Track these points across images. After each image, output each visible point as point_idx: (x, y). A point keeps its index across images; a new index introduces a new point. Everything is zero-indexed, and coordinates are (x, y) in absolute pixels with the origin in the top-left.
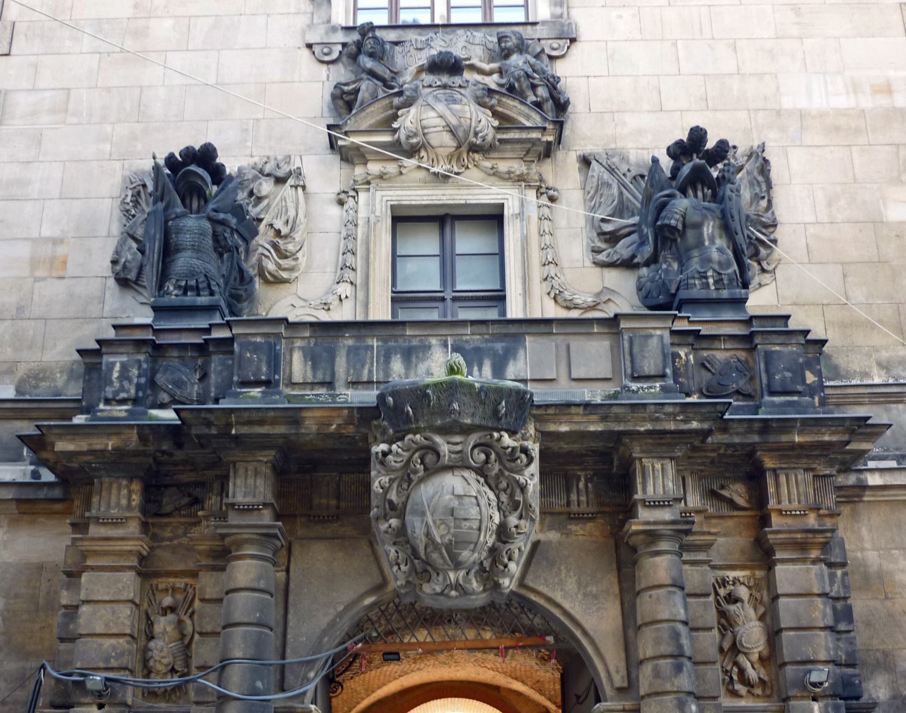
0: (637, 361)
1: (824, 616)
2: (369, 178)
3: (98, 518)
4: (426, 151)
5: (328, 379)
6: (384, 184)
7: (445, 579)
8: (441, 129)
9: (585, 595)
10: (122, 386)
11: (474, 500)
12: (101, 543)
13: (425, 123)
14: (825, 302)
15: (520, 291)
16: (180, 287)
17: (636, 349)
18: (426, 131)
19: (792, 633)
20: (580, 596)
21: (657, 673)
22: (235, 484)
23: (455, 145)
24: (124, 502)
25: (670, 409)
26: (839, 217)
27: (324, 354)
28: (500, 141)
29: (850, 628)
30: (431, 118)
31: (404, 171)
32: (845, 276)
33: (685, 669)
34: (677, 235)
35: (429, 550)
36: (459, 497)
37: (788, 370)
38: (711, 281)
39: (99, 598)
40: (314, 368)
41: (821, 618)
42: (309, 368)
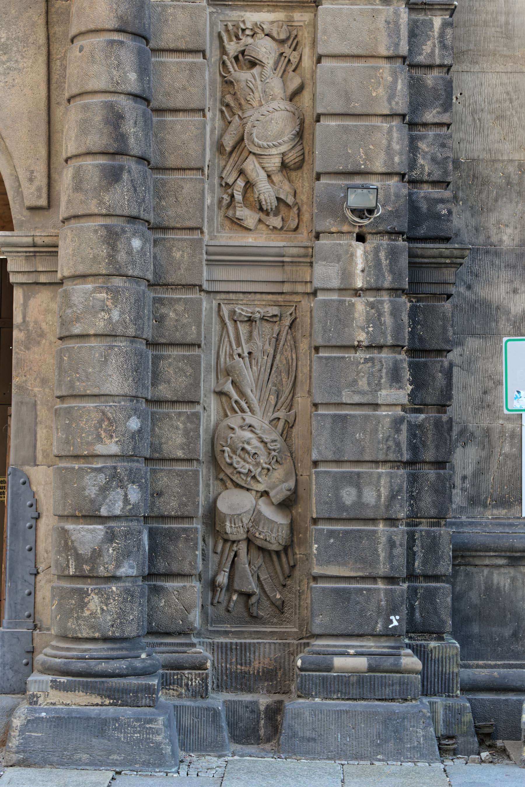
1: (391, 97)
19: (333, 123)
29: (445, 118)
33: (125, 176)
41: (385, 98)
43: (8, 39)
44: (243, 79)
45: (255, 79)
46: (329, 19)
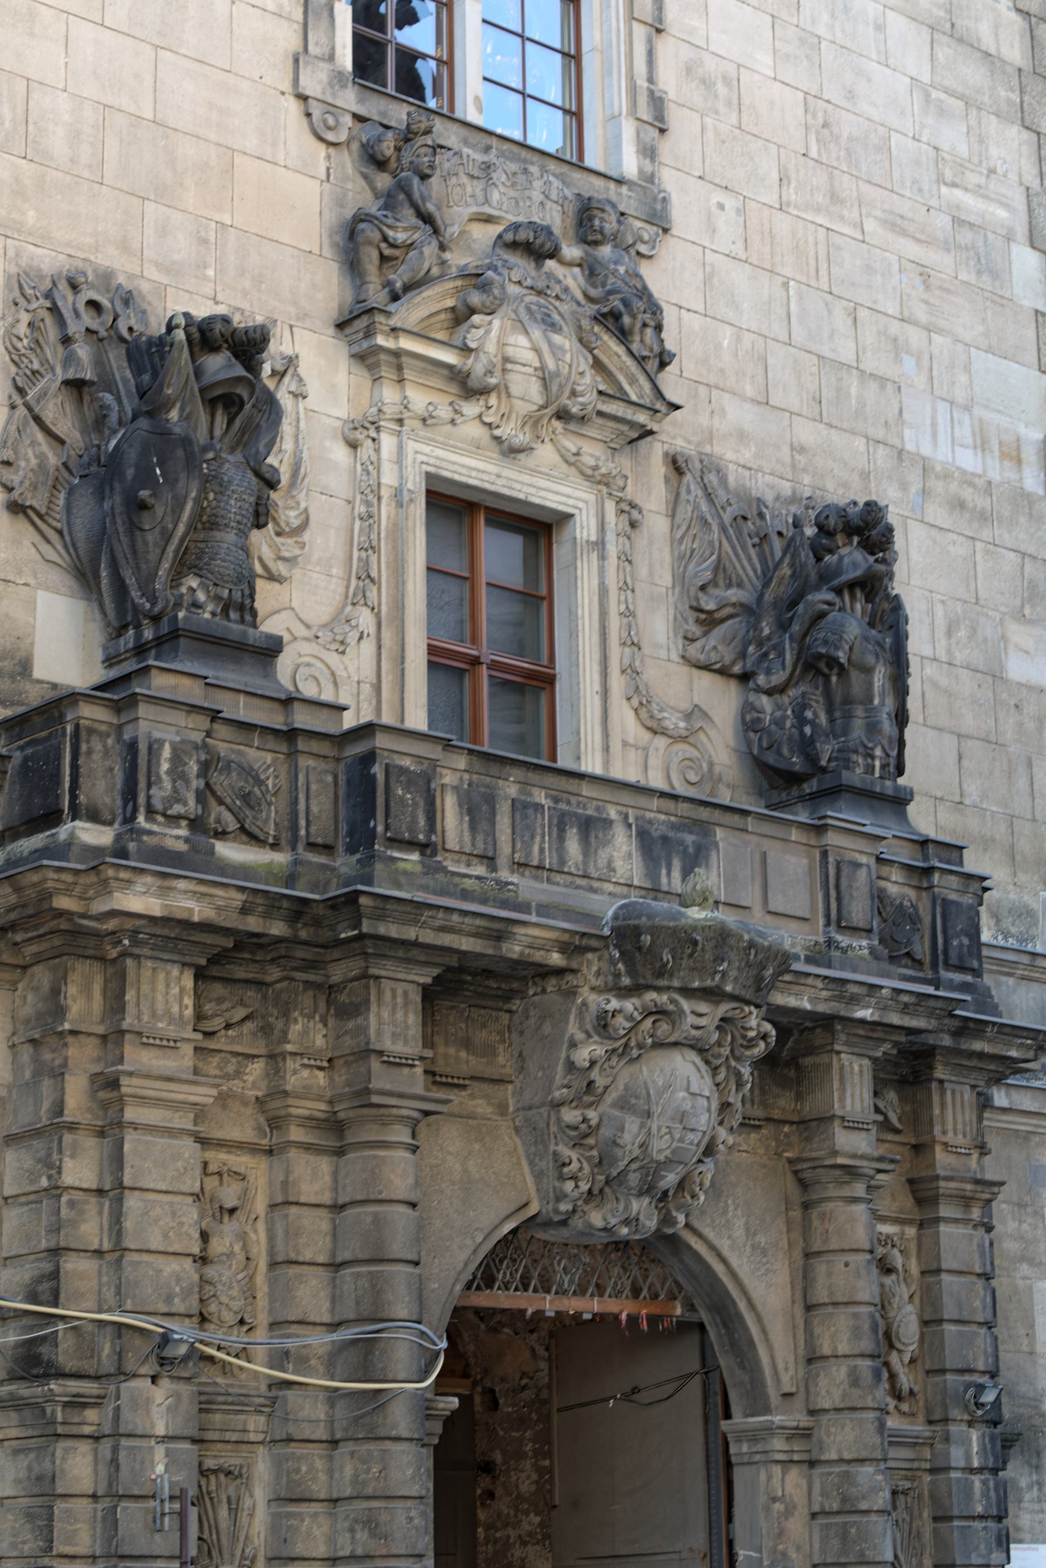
0: (845, 901)
2: (406, 415)
3: (139, 1034)
4: (499, 398)
5: (490, 854)
6: (423, 432)
7: (626, 1207)
8: (530, 370)
9: (753, 1247)
10: (175, 790)
11: (705, 1103)
12: (158, 1084)
13: (510, 351)
14: (939, 794)
15: (597, 687)
16: (217, 598)
17: (844, 882)
18: (509, 366)
20: (748, 1249)
21: (855, 1381)
22: (379, 1015)
23: (541, 402)
24: (175, 1009)
25: (905, 998)
26: (959, 657)
27: (485, 808)
28: (600, 414)
30: (520, 346)
31: (459, 420)
32: (960, 757)
34: (835, 671)
35: (634, 1166)
36: (693, 1094)
38: (877, 763)
39: (152, 1186)
40: (473, 828)
42: (466, 826)
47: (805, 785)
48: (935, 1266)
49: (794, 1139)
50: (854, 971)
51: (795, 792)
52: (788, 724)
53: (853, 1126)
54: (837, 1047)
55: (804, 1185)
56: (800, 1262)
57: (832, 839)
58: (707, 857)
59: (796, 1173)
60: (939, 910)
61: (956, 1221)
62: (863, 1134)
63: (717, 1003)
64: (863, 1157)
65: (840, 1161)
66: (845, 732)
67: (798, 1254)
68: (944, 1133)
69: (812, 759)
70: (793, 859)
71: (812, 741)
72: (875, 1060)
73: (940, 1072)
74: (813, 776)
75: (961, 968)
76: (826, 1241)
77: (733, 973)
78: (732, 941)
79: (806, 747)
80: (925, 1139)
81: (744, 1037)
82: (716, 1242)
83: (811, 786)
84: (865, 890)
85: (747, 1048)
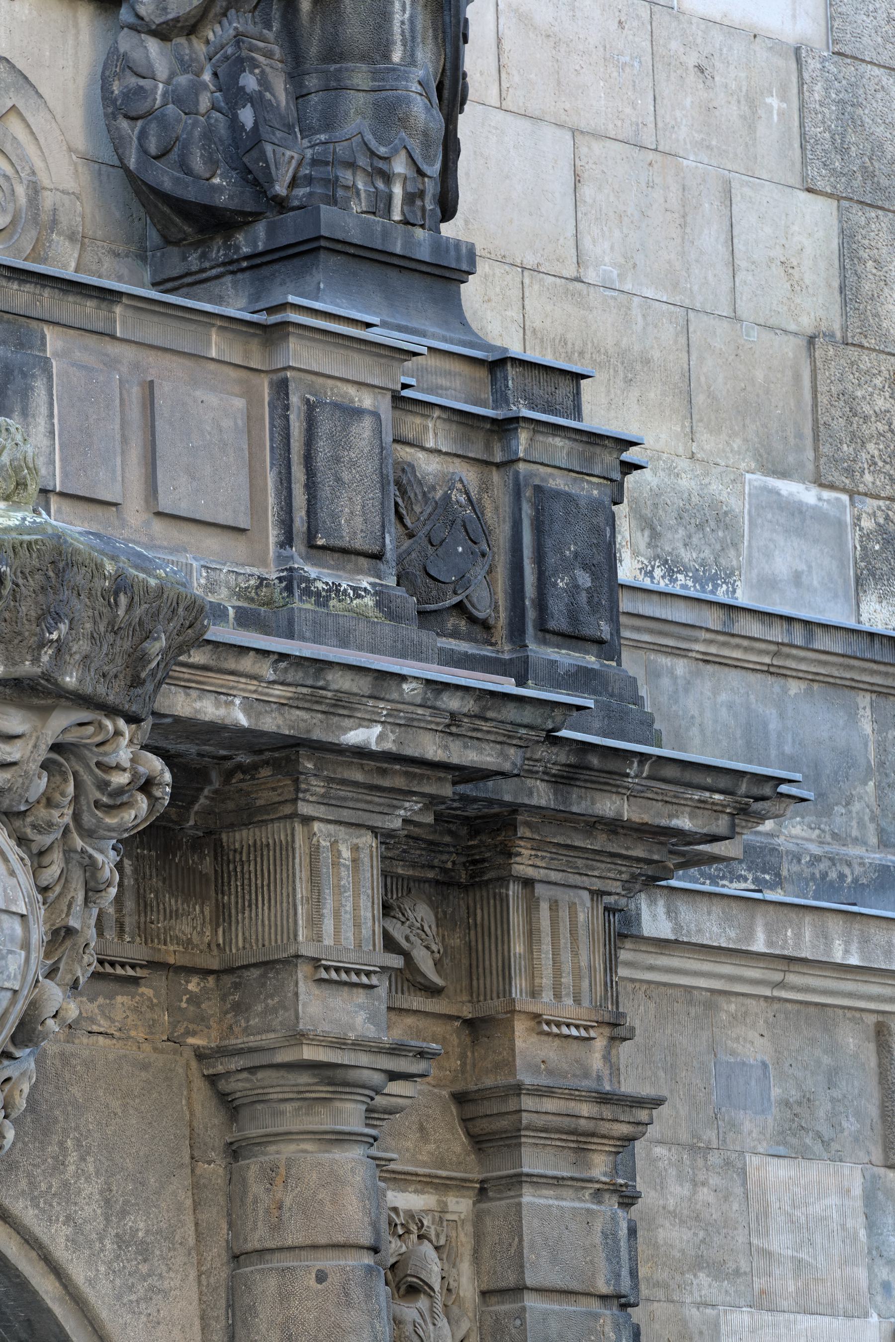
0: (325, 492)
9: (120, 1240)
14: (530, 260)
25: (453, 703)
32: (577, 180)
37: (585, 567)
38: (398, 191)
43: (147, 1232)
44: (409, 1319)
45: (424, 1321)
46: (536, 1223)
47: (240, 238)
48: (511, 1280)
49: (211, 1007)
50: (344, 643)
51: (218, 252)
52: (204, 103)
53: (336, 977)
54: (304, 809)
55: (231, 1106)
56: (221, 1274)
57: (299, 354)
58: (25, 393)
59: (212, 1080)
60: (527, 510)
61: (557, 1182)
62: (360, 997)
63: (45, 711)
64: (358, 1045)
65: (309, 1053)
66: (329, 122)
67: (216, 1254)
68: (534, 993)
69: (256, 181)
70: (213, 399)
71: (256, 139)
72: (385, 837)
73: (525, 864)
74: (257, 216)
75: (573, 638)
76: (276, 1227)
77: (81, 647)
78: (79, 578)
79: (244, 154)
80: (493, 1006)
81: (103, 786)
82: (39, 1230)
83: (253, 239)
84: (369, 467)
85: (109, 808)
